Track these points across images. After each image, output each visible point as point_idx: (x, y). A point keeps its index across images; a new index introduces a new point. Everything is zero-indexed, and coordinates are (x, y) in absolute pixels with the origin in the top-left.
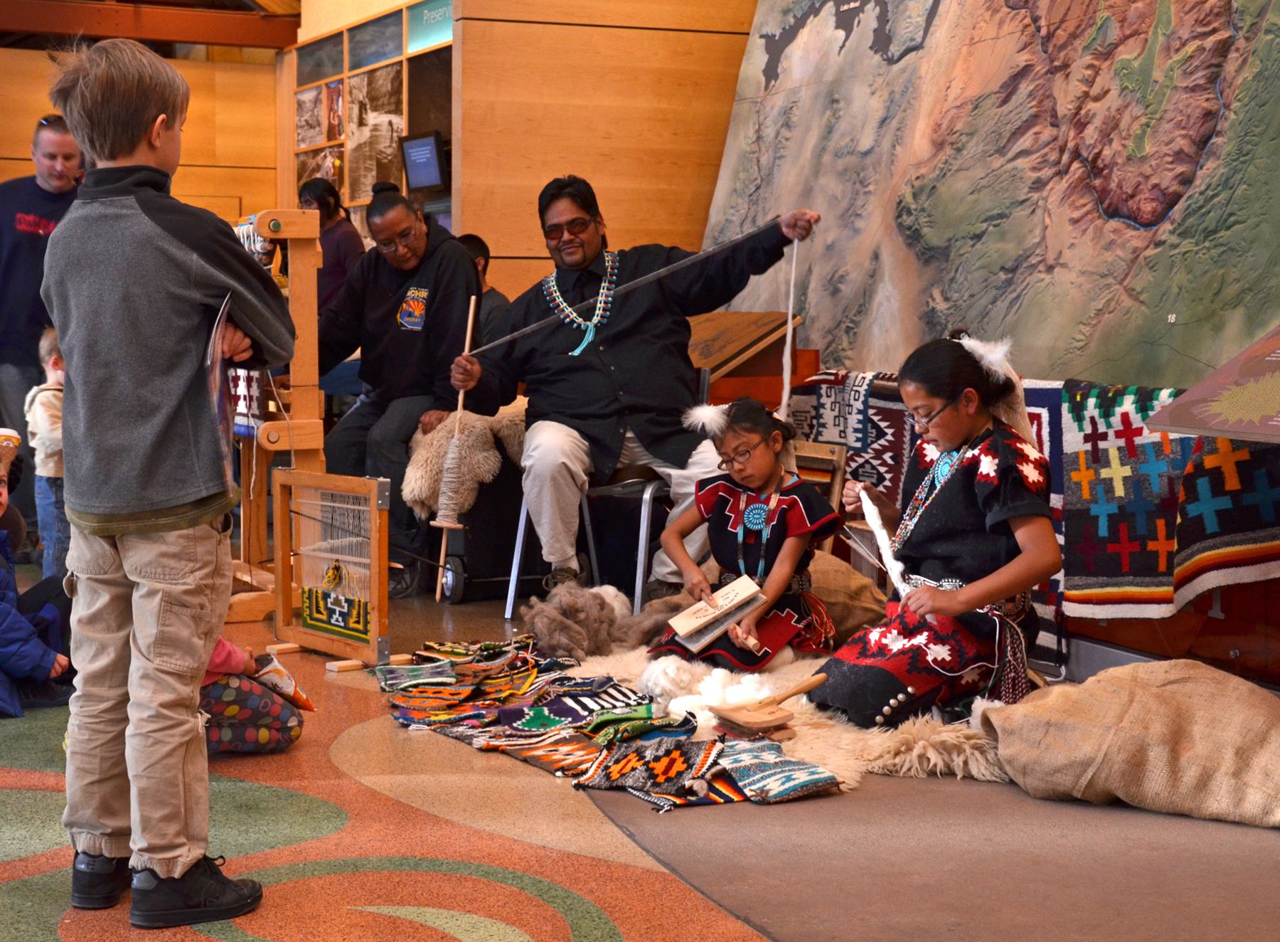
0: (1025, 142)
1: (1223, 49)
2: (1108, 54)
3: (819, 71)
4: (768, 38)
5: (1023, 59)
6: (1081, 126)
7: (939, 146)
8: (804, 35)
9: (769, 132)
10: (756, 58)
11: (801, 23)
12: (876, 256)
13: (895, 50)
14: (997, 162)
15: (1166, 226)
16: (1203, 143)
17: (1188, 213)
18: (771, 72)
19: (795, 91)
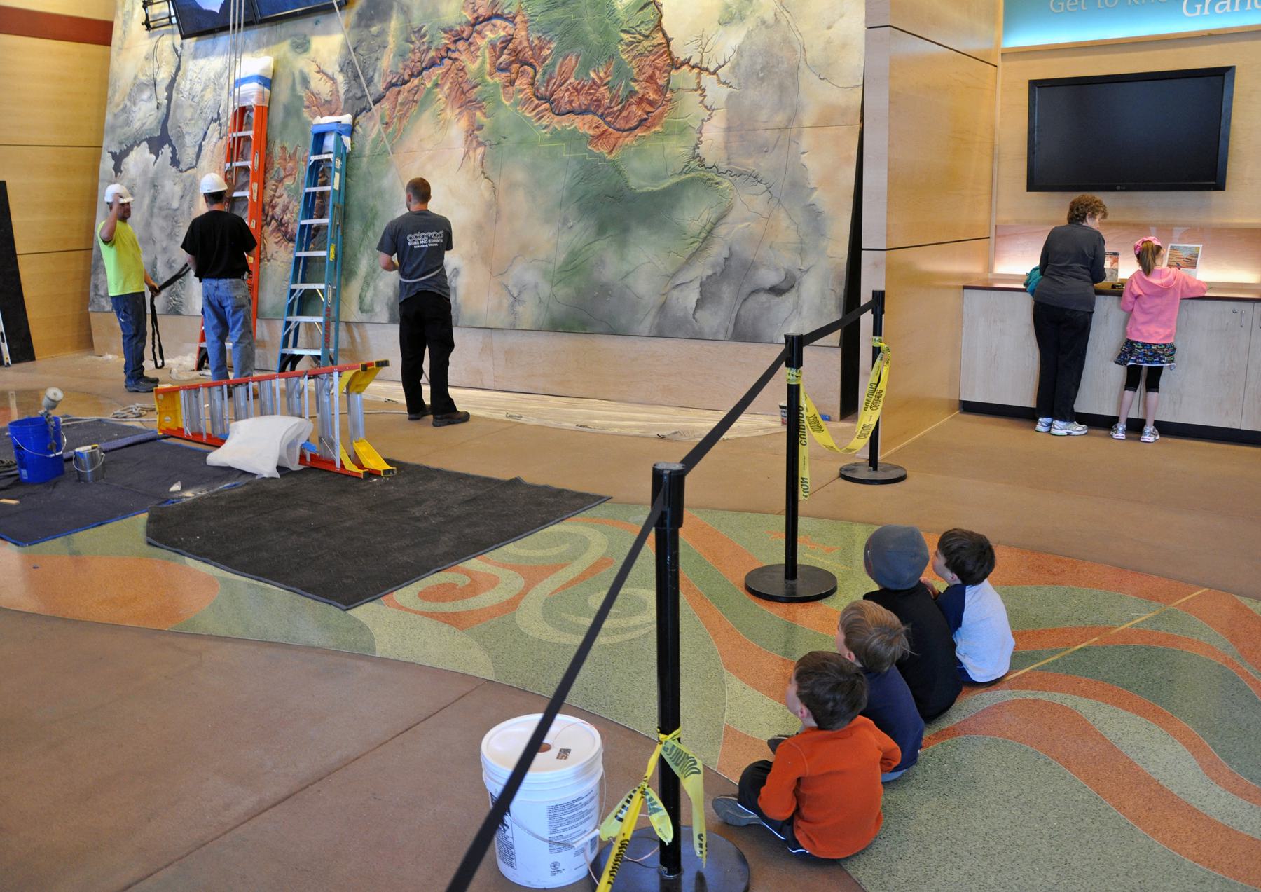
2: (281, 181)
3: (145, 172)
4: (114, 155)
6: (274, 207)
10: (107, 163)
11: (130, 149)
13: (182, 166)
18: (117, 169)
19: (133, 180)
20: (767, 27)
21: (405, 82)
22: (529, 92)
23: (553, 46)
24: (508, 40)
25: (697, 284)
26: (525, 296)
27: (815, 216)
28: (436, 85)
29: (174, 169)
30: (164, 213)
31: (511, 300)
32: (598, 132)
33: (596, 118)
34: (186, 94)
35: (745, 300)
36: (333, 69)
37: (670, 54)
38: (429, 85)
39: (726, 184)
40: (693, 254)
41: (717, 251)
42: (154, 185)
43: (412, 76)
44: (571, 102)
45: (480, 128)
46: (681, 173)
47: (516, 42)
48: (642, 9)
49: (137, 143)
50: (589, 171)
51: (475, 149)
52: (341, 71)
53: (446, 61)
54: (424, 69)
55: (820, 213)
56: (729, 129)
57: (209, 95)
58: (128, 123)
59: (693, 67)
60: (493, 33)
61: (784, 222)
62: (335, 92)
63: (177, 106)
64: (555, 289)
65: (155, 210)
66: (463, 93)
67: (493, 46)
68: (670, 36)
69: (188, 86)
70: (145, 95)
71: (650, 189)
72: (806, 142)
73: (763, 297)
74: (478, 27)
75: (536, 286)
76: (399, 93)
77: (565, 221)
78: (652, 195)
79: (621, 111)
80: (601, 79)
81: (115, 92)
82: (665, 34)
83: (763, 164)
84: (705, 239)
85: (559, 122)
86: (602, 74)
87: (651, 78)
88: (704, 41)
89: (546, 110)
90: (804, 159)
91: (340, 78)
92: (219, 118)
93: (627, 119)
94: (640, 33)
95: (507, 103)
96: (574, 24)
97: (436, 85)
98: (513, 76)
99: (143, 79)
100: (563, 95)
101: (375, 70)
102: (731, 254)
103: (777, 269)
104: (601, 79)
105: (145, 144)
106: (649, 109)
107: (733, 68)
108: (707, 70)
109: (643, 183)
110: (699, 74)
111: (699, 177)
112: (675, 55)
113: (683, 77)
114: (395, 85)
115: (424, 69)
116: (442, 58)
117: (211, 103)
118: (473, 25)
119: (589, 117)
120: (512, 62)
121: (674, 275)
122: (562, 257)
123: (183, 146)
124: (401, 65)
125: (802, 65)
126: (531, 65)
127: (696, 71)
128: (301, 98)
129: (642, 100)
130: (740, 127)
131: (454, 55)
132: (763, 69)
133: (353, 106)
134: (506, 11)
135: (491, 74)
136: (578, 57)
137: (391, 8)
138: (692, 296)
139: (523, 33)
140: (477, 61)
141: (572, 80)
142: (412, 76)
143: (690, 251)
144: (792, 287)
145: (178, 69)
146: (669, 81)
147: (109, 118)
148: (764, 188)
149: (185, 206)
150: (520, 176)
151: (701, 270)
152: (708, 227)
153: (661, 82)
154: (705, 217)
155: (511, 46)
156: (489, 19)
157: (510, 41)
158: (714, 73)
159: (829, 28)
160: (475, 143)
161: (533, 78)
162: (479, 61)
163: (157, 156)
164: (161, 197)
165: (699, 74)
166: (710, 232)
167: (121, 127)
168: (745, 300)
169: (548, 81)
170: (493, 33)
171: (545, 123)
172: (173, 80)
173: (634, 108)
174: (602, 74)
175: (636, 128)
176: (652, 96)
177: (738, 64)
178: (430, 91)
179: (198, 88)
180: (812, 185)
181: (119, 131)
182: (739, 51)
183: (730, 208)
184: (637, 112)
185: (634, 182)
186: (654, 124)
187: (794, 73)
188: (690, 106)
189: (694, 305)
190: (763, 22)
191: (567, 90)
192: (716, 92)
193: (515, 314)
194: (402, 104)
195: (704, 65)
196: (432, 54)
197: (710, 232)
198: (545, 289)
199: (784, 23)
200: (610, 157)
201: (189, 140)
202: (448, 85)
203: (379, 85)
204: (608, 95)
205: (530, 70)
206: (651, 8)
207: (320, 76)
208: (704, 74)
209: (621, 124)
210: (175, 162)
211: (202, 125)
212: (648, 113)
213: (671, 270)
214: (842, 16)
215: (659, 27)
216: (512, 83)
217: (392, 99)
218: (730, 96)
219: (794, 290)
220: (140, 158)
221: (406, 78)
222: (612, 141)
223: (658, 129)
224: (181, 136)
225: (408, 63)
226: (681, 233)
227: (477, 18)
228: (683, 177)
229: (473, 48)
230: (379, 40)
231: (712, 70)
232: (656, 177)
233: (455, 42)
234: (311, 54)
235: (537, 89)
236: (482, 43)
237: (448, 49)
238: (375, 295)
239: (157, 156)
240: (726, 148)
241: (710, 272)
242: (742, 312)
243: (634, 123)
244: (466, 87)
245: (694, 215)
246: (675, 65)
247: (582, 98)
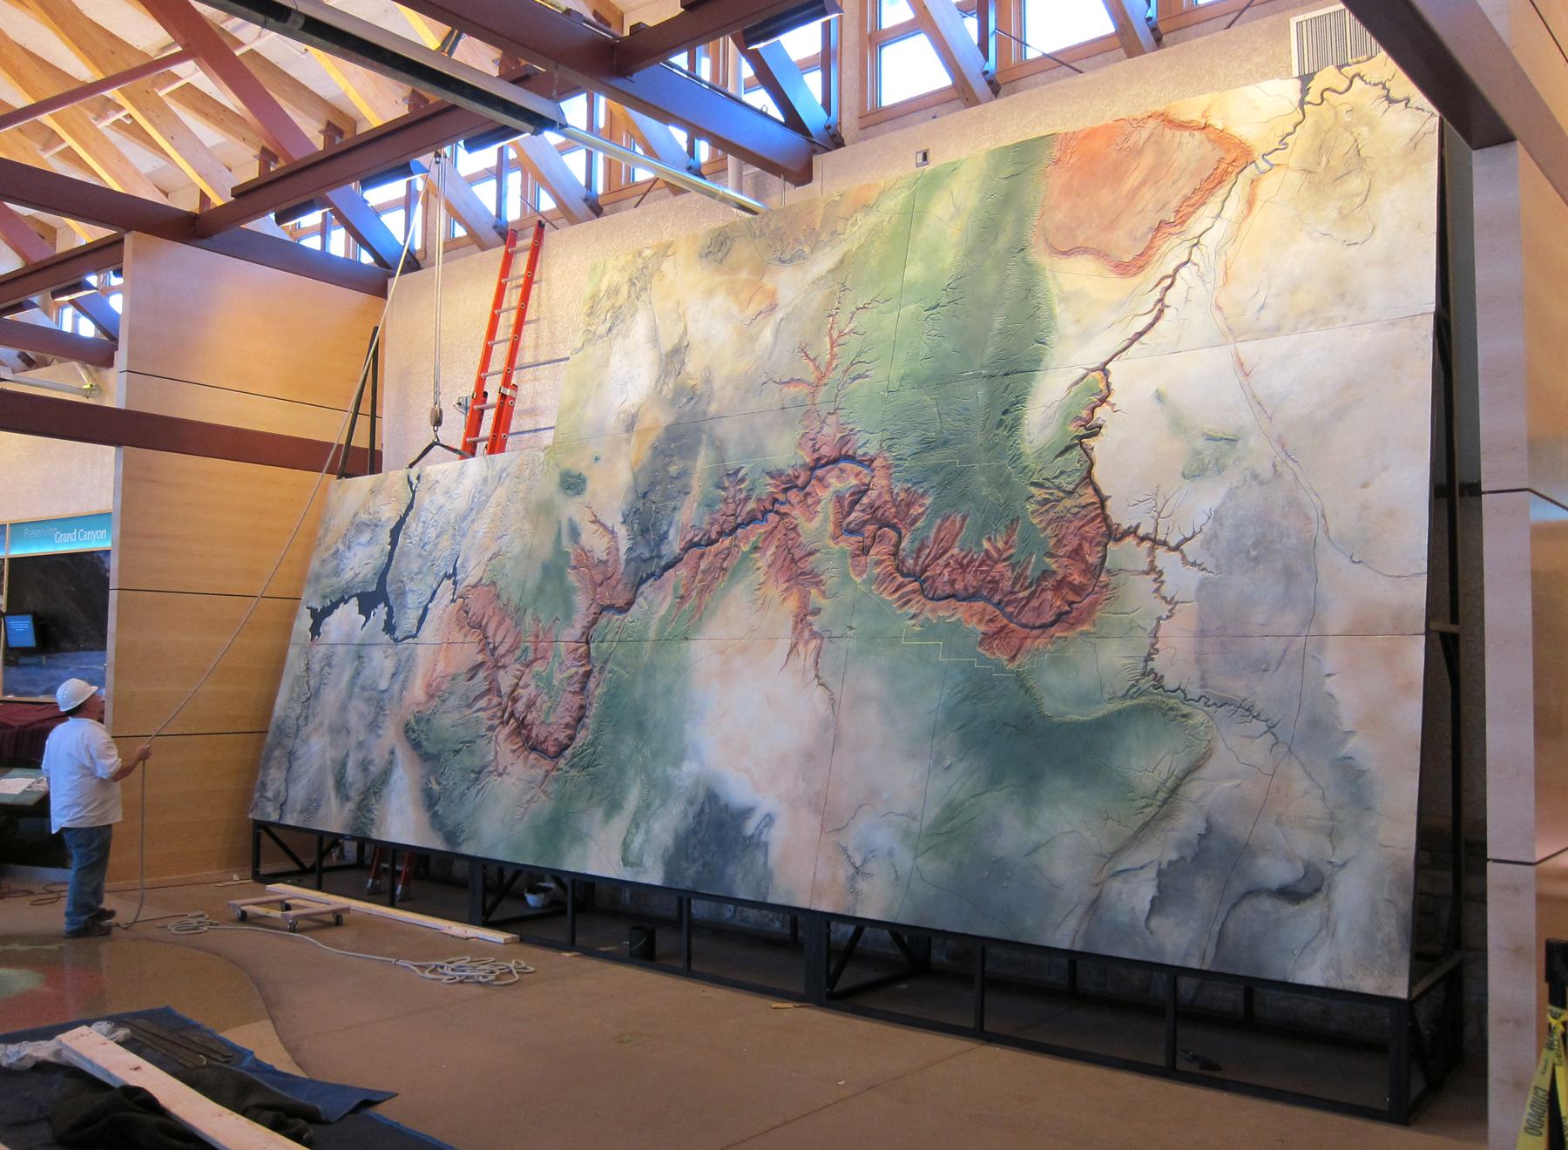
0: (483, 703)
1: (588, 674)
2: (528, 665)
4: (314, 612)
5: (480, 658)
6: (515, 701)
7: (431, 696)
8: (337, 613)
9: (316, 667)
10: (304, 621)
11: (335, 606)
12: (392, 752)
13: (398, 634)
14: (467, 712)
15: (562, 763)
16: (579, 720)
17: (574, 756)
18: (315, 630)
20: (1262, 483)
21: (711, 543)
22: (889, 564)
23: (928, 501)
24: (861, 492)
25: (1152, 873)
26: (872, 867)
27: (1352, 777)
28: (756, 549)
30: (367, 694)
31: (851, 871)
32: (993, 627)
33: (990, 608)
34: (415, 540)
35: (1234, 905)
36: (614, 520)
37: (1106, 519)
38: (745, 548)
39: (1199, 718)
40: (1146, 825)
41: (1187, 823)
42: (360, 653)
43: (721, 534)
44: (952, 582)
45: (816, 612)
46: (1124, 697)
47: (873, 494)
48: (1062, 453)
49: (344, 600)
50: (978, 687)
51: (807, 643)
52: (624, 522)
53: (771, 516)
54: (739, 526)
55: (1362, 773)
56: (1202, 634)
57: (445, 542)
58: (337, 572)
59: (1143, 539)
60: (840, 482)
61: (1300, 784)
62: (613, 550)
63: (404, 554)
64: (920, 861)
65: (356, 690)
66: (794, 561)
67: (839, 499)
68: (1105, 492)
69: (420, 530)
70: (365, 537)
71: (1075, 717)
72: (1333, 658)
73: (1267, 904)
74: (819, 472)
75: (890, 854)
76: (702, 556)
77: (939, 758)
78: (1080, 726)
79: (1029, 599)
80: (999, 551)
81: (327, 530)
82: (1097, 491)
83: (1261, 691)
84: (1165, 802)
85: (933, 610)
86: (1000, 545)
87: (1077, 553)
88: (1160, 502)
89: (914, 592)
90: (1331, 685)
91: (622, 532)
92: (455, 574)
93: (1038, 611)
94: (1059, 488)
95: (858, 580)
96: (961, 473)
97: (756, 549)
98: (868, 542)
99: (364, 517)
100: (941, 574)
101: (670, 525)
102: (1210, 828)
103: (1290, 860)
104: (999, 551)
105: (354, 601)
106: (1071, 597)
107: (1207, 543)
108: (1164, 543)
109: (1062, 707)
110: (1152, 549)
111: (1152, 704)
112: (1115, 519)
113: (1124, 554)
114: (698, 545)
115: (739, 526)
116: (765, 512)
117: (447, 553)
118: (813, 469)
119: (979, 605)
120: (865, 523)
121: (1114, 855)
122: (932, 813)
123: (403, 606)
124: (707, 519)
125: (1321, 540)
126: (893, 527)
127: (1147, 544)
128: (567, 554)
129: (1061, 584)
130: (1220, 632)
131: (783, 509)
132: (1256, 545)
133: (636, 575)
134: (860, 452)
135: (835, 538)
136: (964, 519)
137: (699, 443)
138: (1142, 892)
139: (884, 482)
140: (816, 523)
141: (955, 551)
142: (721, 534)
143: (1139, 821)
144: (1318, 890)
145: (410, 507)
146: (1104, 557)
147: (315, 564)
148: (1263, 727)
149: (396, 688)
150: (872, 684)
151: (1159, 851)
152: (1169, 784)
153: (1093, 559)
154: (1164, 769)
155: (865, 500)
156: (835, 461)
157: (864, 493)
158: (1177, 548)
159: (1365, 486)
160: (806, 634)
161: (897, 545)
162: (819, 517)
164: (366, 673)
165: (1152, 549)
166: (1174, 790)
167: (328, 576)
168: (1234, 905)
169: (920, 550)
170: (840, 482)
171: (913, 611)
172: (402, 521)
173: (1049, 595)
174: (1000, 545)
175: (1052, 624)
176: (1077, 579)
177: (1215, 536)
178: (746, 556)
179: (432, 533)
180: (1347, 726)
181: (325, 581)
182: (1216, 517)
183: (1207, 755)
184: (1053, 603)
185: (1050, 706)
186: (1080, 621)
187: (1309, 550)
188: (1139, 595)
189: (1147, 906)
190: (1255, 476)
191: (948, 565)
192: (1180, 578)
193: (856, 893)
194: (704, 572)
195: (1161, 537)
196: (751, 505)
197: (1174, 790)
198: (905, 860)
199: (1288, 477)
200: (1011, 667)
201: (413, 601)
202: (772, 549)
203: (674, 545)
204: (1009, 574)
205: (893, 534)
206: (1076, 453)
207: (595, 527)
208: (1160, 551)
209: (1028, 617)
210: (389, 627)
211: (431, 581)
212: (1071, 604)
213: (1108, 847)
214: (1386, 468)
215: (1088, 479)
216: (865, 551)
217: (692, 563)
218: (1203, 585)
219: (1320, 897)
220: (346, 617)
221: (714, 536)
222: (1015, 641)
223: (1085, 628)
224: (402, 594)
225: (717, 516)
226: (1124, 789)
227: (819, 459)
228: (1128, 703)
229: (810, 501)
230: (677, 482)
231: (1173, 544)
232: (1083, 700)
233: (785, 490)
234: (586, 497)
235: (903, 561)
236: (826, 495)
237: (775, 501)
238: (646, 841)
240: (1198, 661)
241: (1174, 856)
242: (1231, 926)
243: (1049, 617)
244: (798, 554)
245: (1148, 763)
246: (1113, 534)
247: (970, 577)
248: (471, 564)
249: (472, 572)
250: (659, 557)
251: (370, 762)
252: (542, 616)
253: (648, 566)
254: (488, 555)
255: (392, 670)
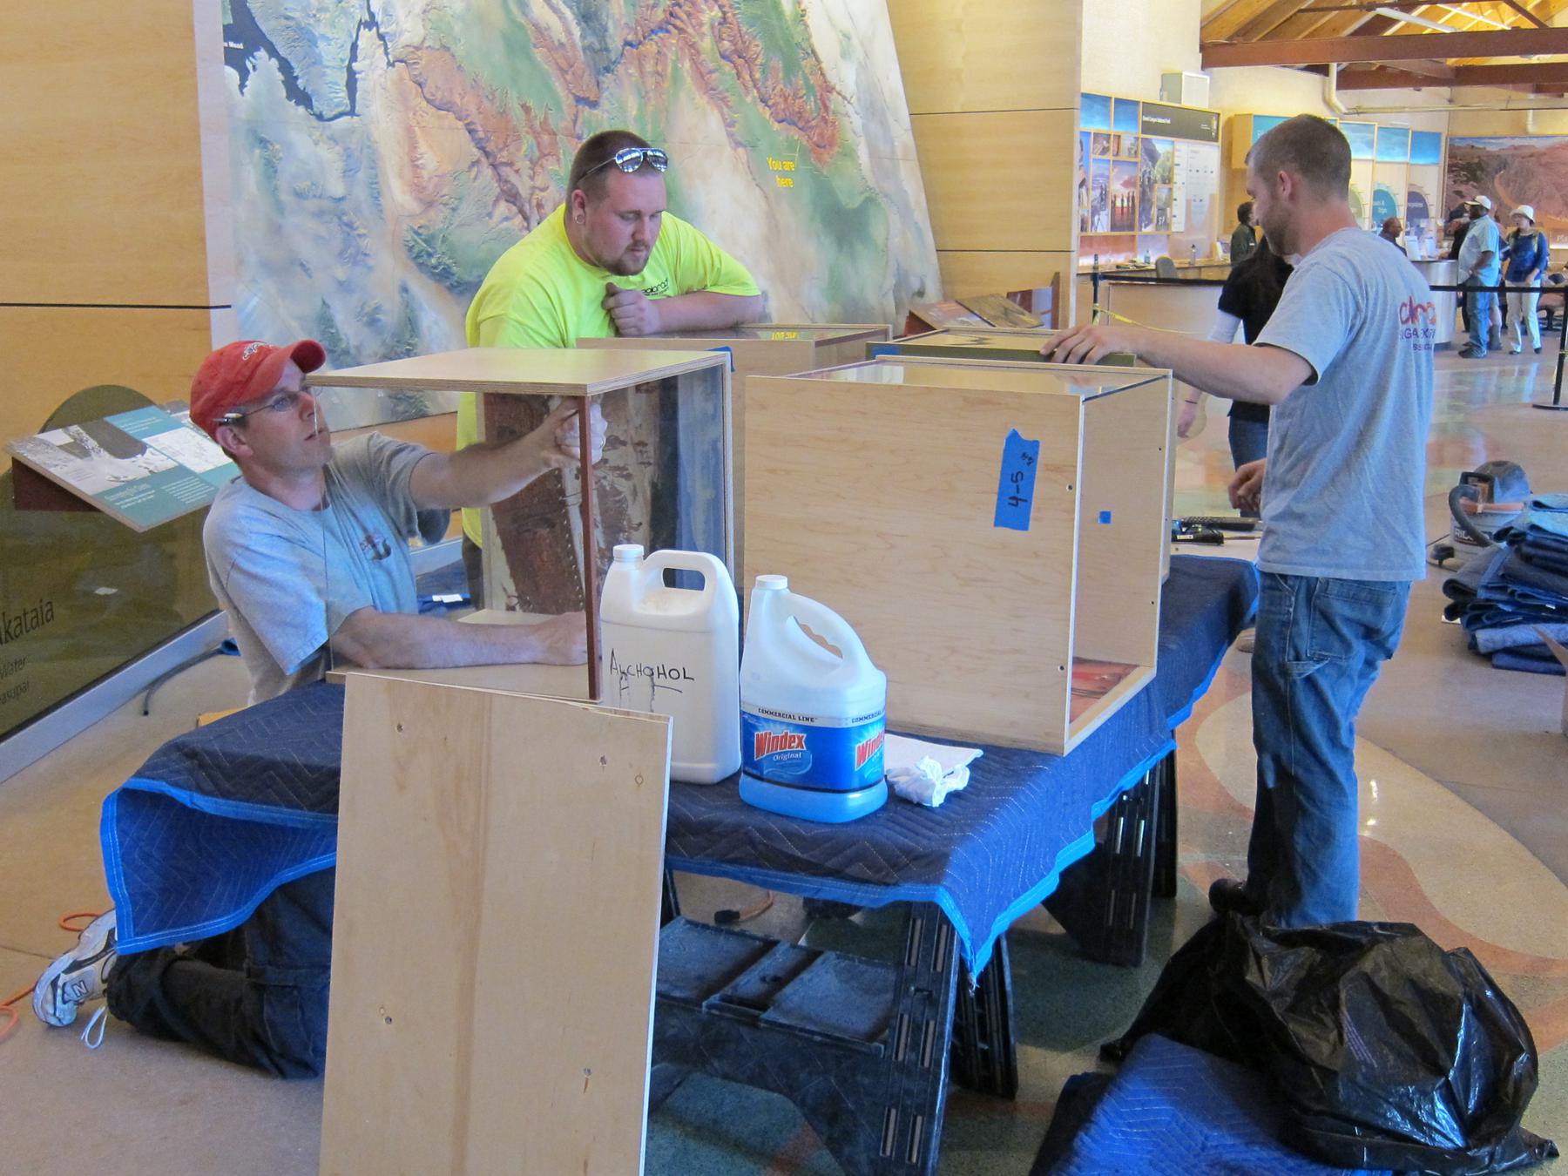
12: (405, 290)
29: (301, 109)
30: (312, 205)
149: (360, 193)
163: (244, 74)
201: (332, 53)
224: (305, 37)
239: (244, 74)
248: (400, 13)
249: (408, 28)
250: (607, 50)
251: (377, 309)
252: (530, 104)
253: (602, 63)
254: (418, 9)
255: (340, 165)
